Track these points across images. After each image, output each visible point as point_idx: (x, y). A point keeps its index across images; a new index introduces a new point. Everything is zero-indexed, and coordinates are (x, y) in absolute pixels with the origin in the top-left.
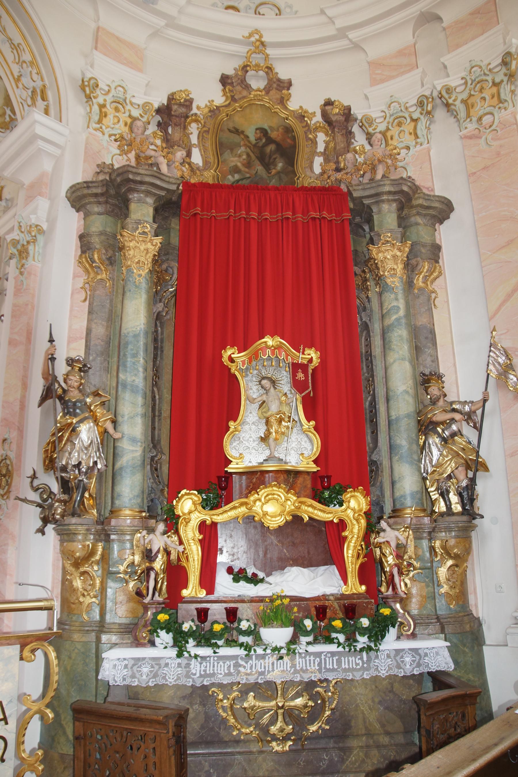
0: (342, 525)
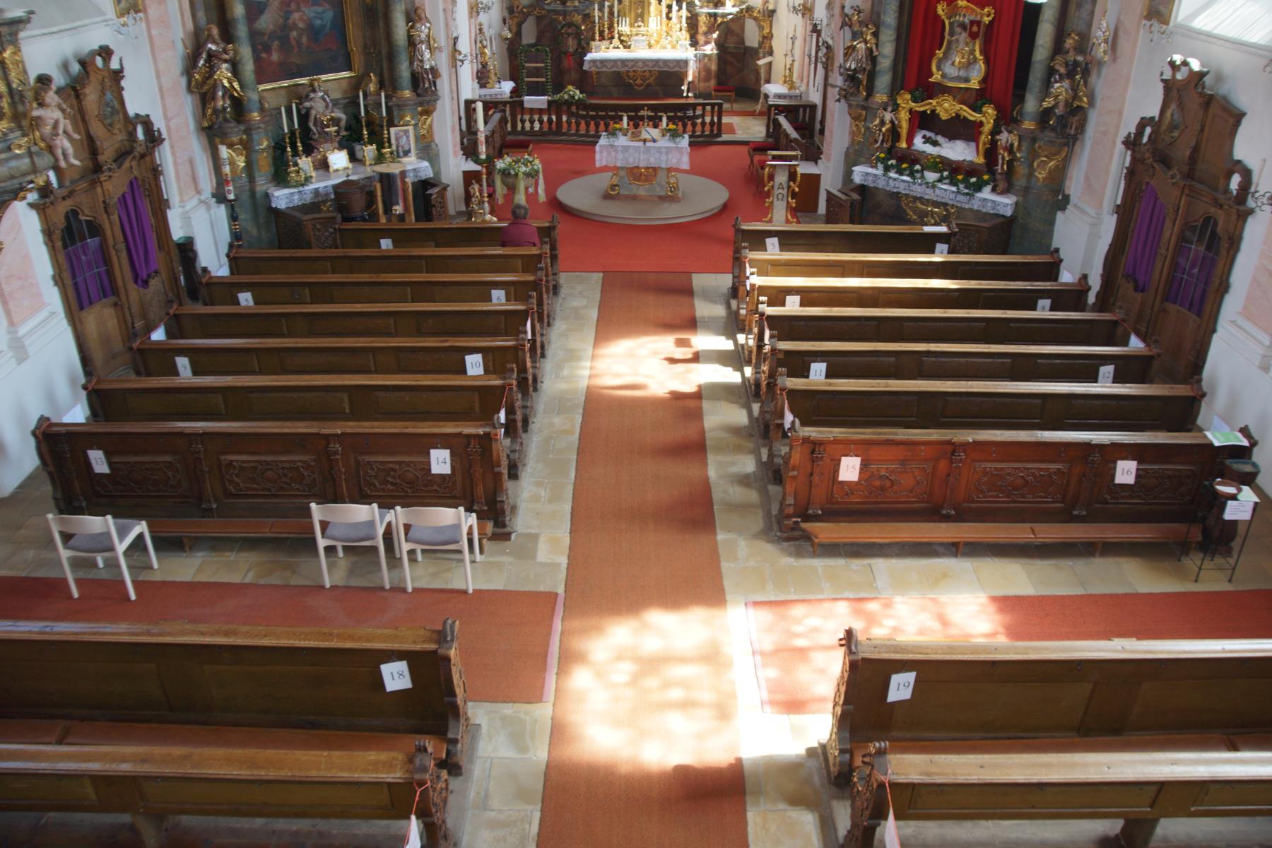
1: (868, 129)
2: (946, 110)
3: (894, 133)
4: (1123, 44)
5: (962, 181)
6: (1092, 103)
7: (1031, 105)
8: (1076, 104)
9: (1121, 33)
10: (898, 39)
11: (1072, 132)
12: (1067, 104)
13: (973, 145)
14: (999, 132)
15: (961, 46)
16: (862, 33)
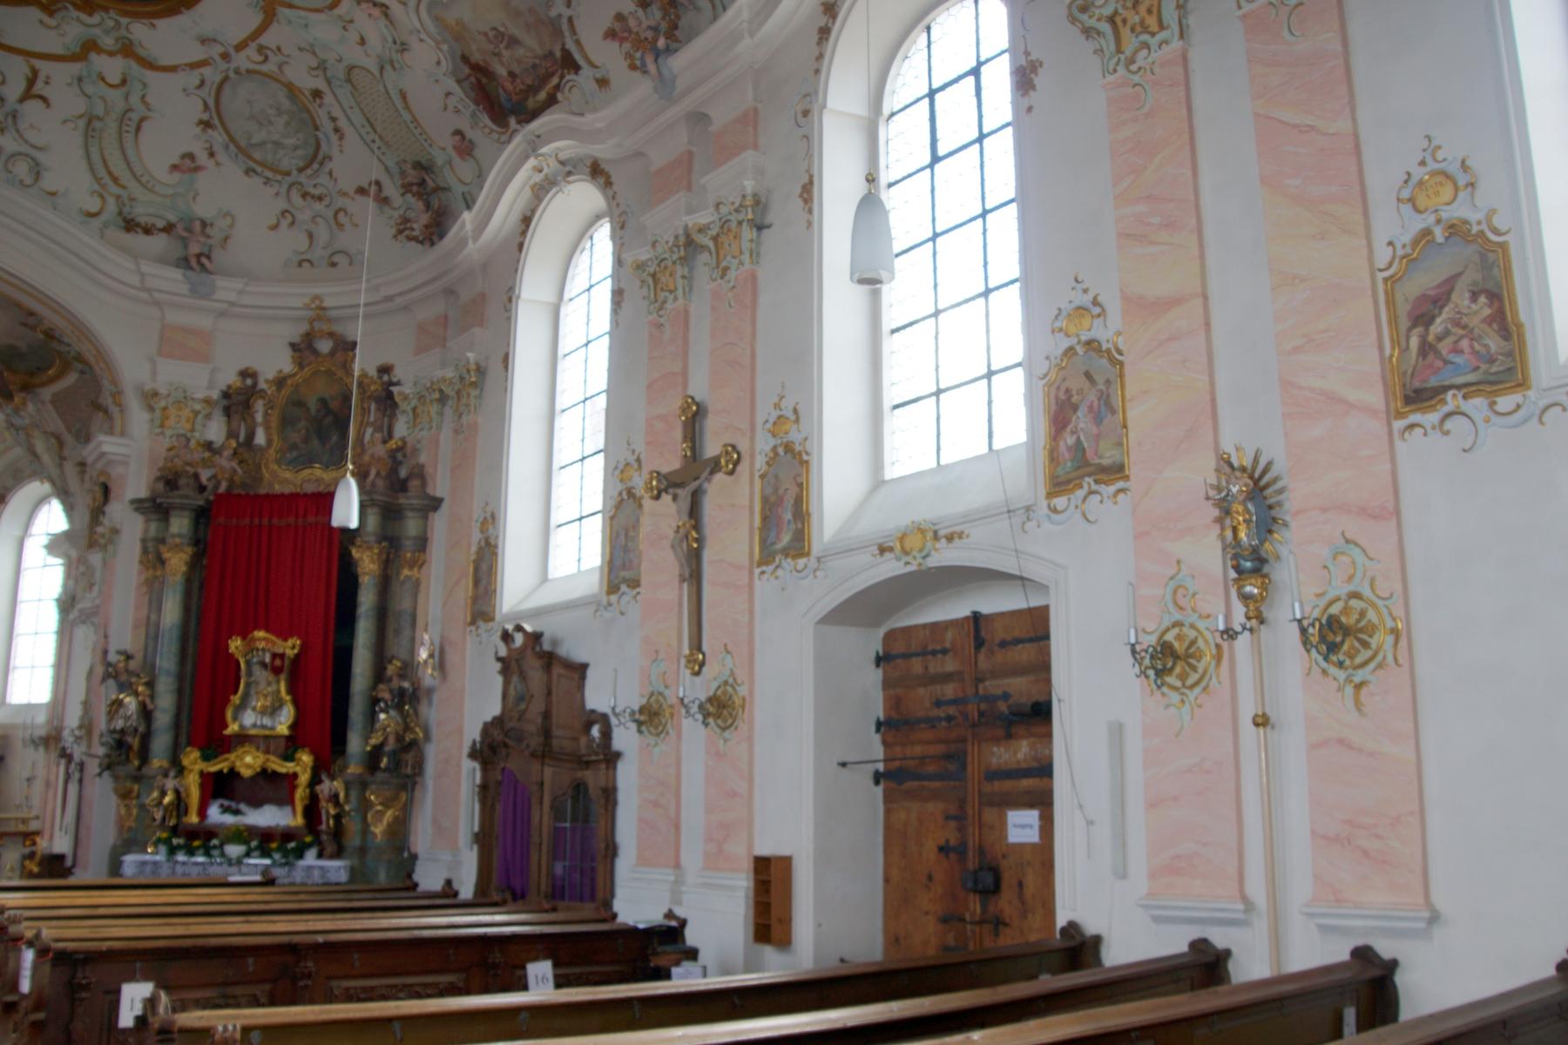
0: (295, 776)
1: (142, 807)
2: (248, 766)
3: (180, 805)
4: (452, 658)
5: (279, 849)
6: (427, 738)
7: (356, 744)
8: (408, 737)
9: (448, 649)
10: (180, 691)
11: (409, 771)
12: (399, 738)
13: (288, 809)
14: (320, 782)
15: (262, 685)
16: (131, 684)
